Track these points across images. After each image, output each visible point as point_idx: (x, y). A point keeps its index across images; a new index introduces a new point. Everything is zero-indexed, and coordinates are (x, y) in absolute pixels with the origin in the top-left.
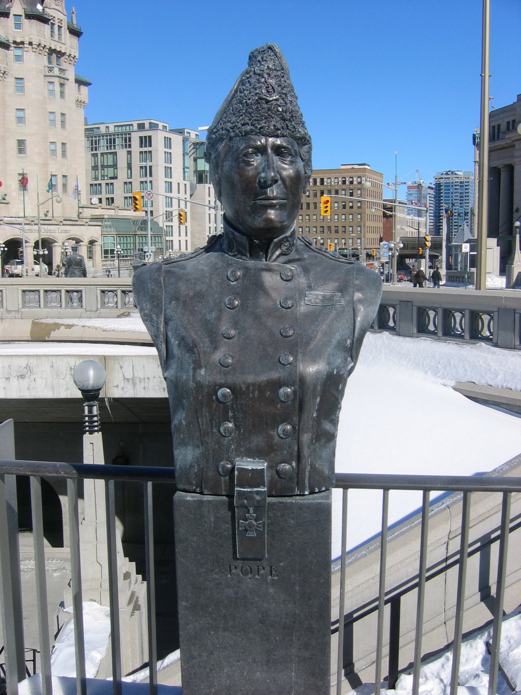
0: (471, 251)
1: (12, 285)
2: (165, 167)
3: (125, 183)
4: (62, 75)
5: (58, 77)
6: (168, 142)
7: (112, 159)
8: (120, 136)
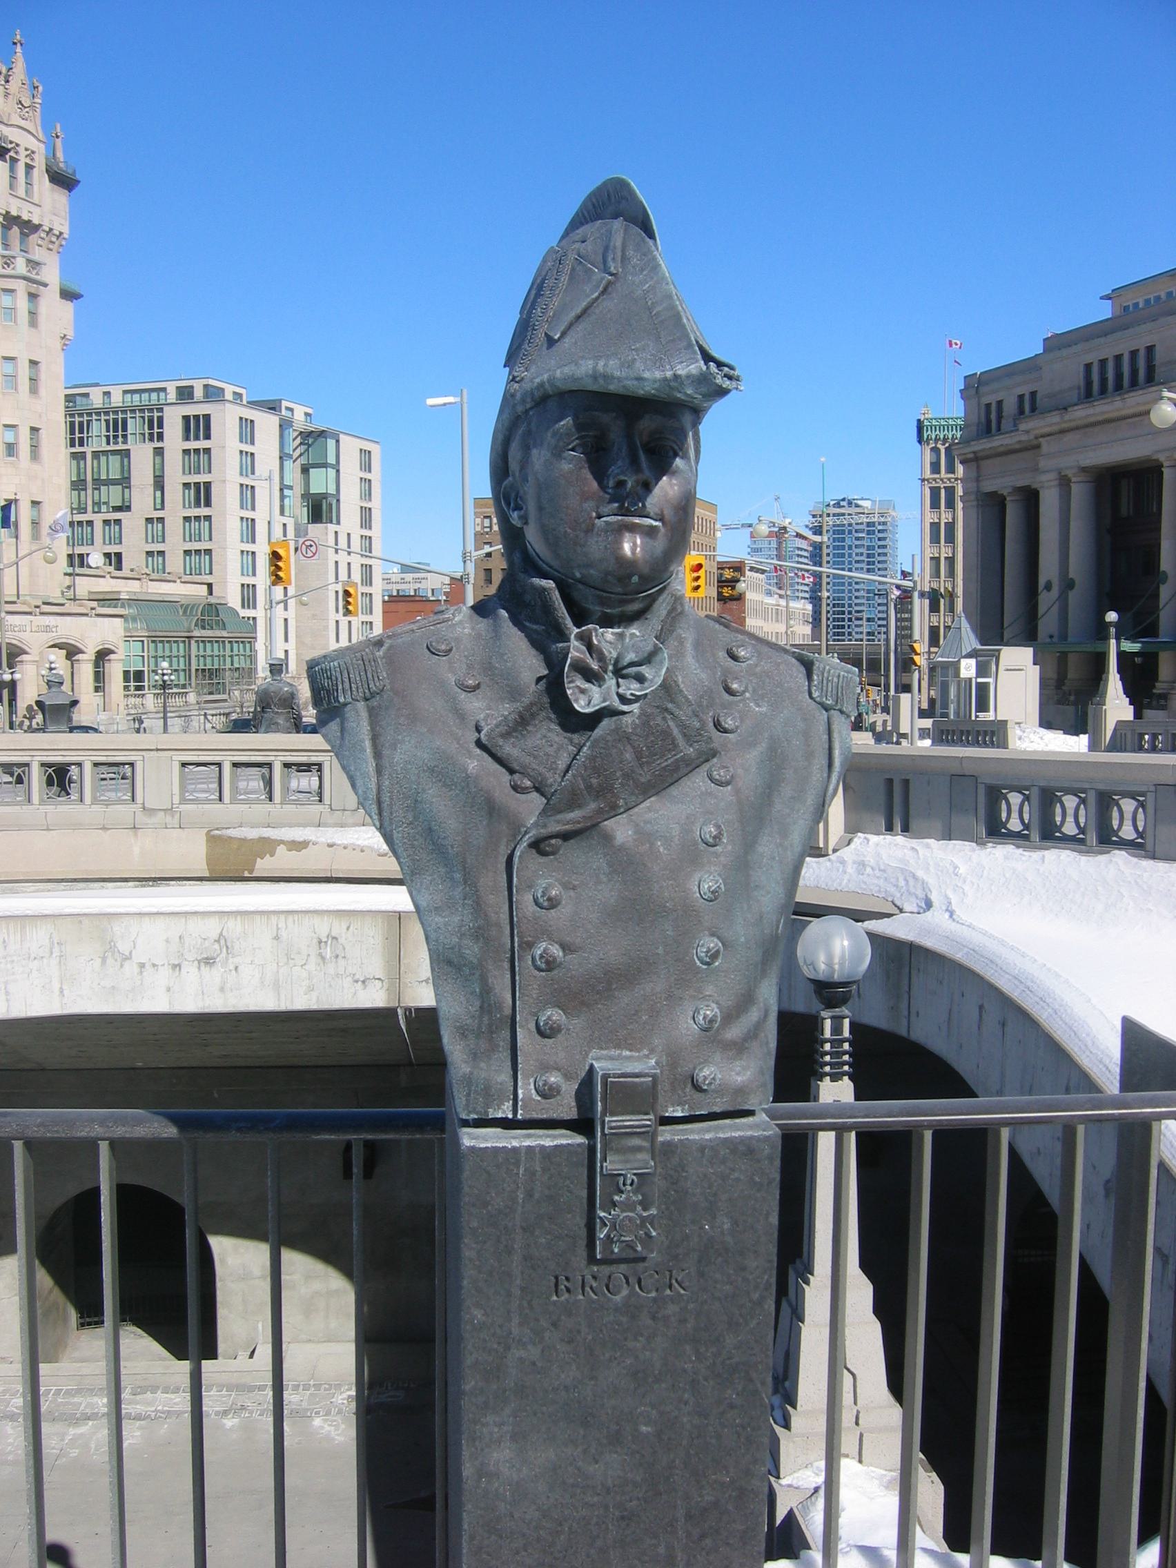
0: (978, 676)
1: (158, 750)
2: (242, 485)
3: (150, 520)
4: (33, 276)
5: (25, 278)
6: (247, 429)
7: (118, 465)
8: (138, 414)
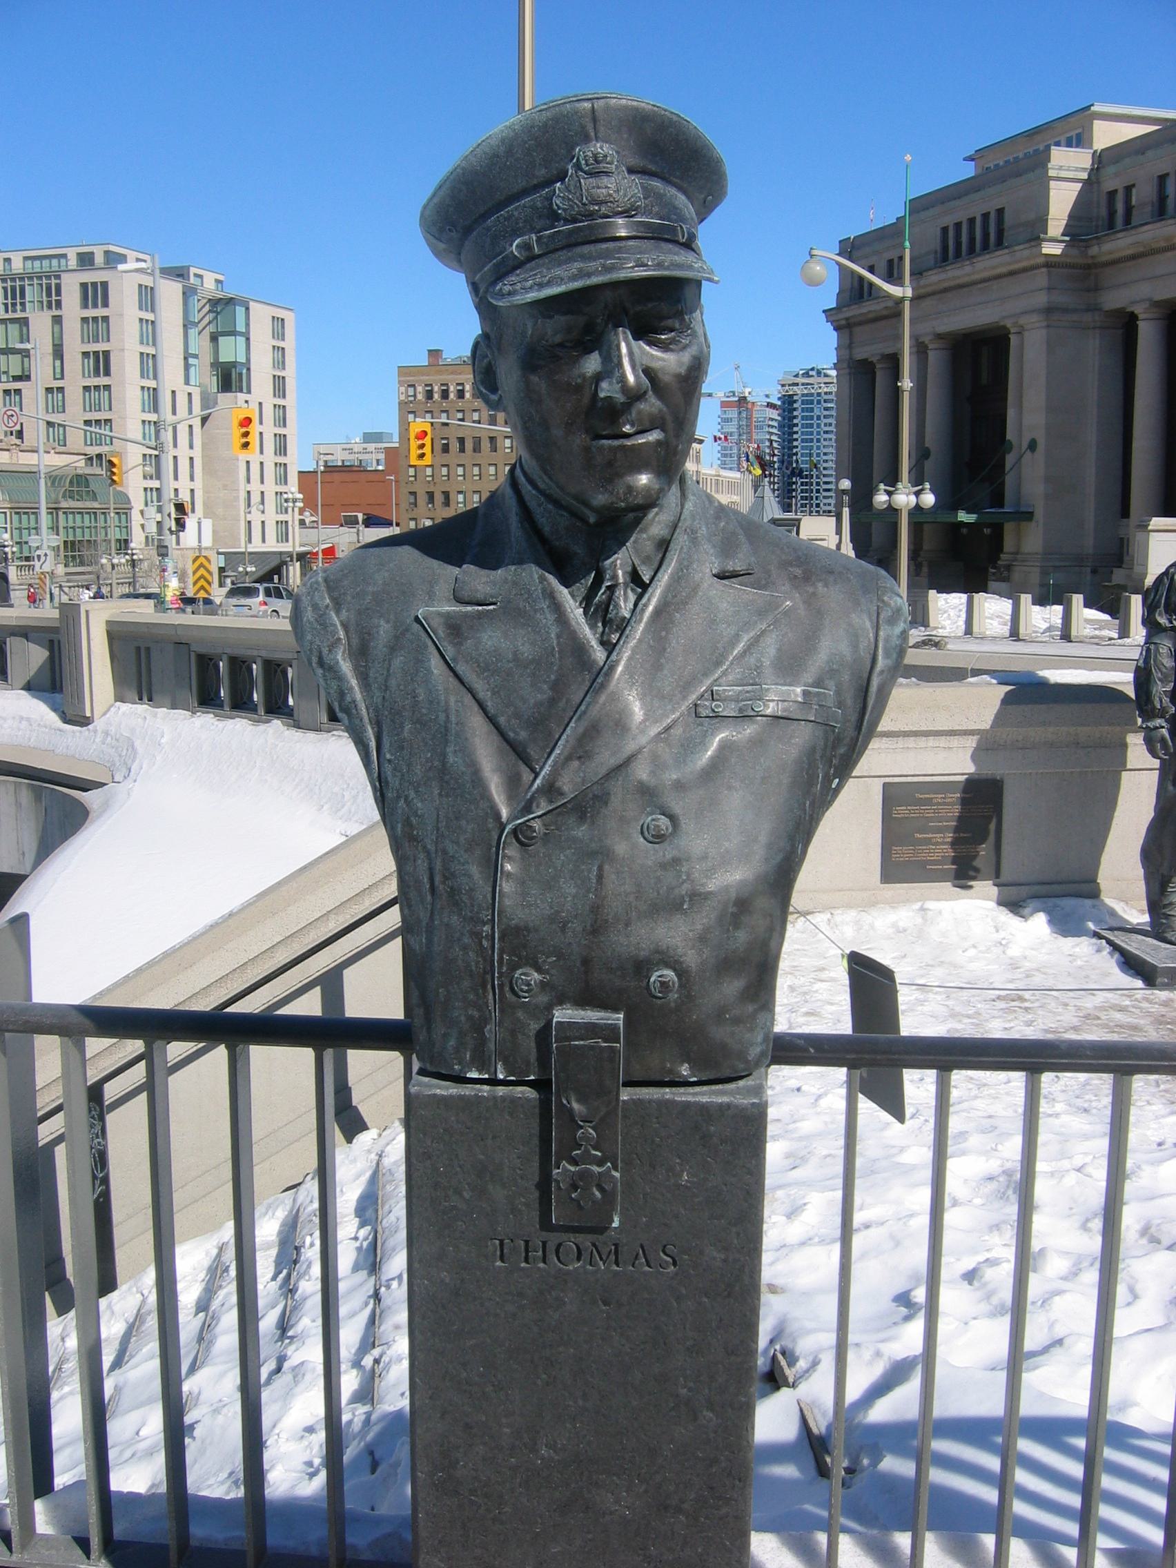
2: (142, 354)
6: (147, 297)
7: (17, 333)
8: (36, 281)
